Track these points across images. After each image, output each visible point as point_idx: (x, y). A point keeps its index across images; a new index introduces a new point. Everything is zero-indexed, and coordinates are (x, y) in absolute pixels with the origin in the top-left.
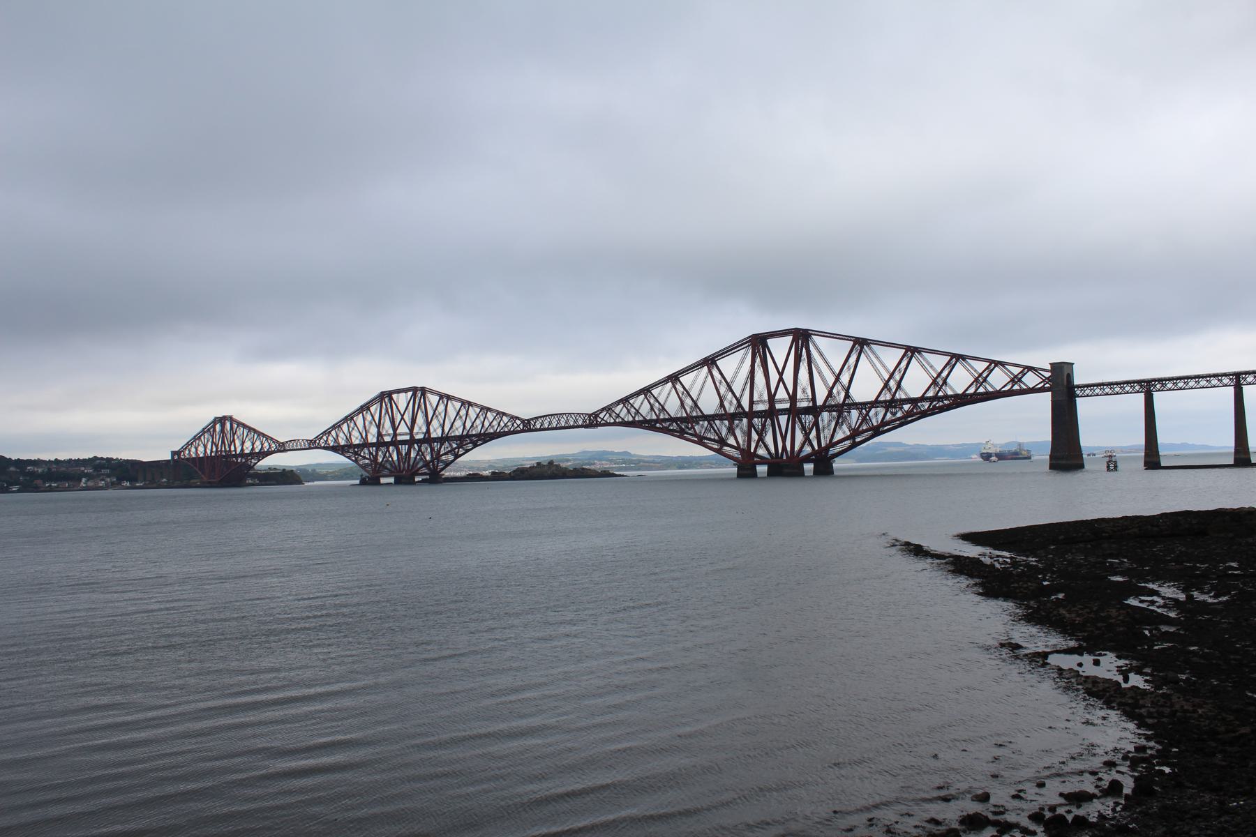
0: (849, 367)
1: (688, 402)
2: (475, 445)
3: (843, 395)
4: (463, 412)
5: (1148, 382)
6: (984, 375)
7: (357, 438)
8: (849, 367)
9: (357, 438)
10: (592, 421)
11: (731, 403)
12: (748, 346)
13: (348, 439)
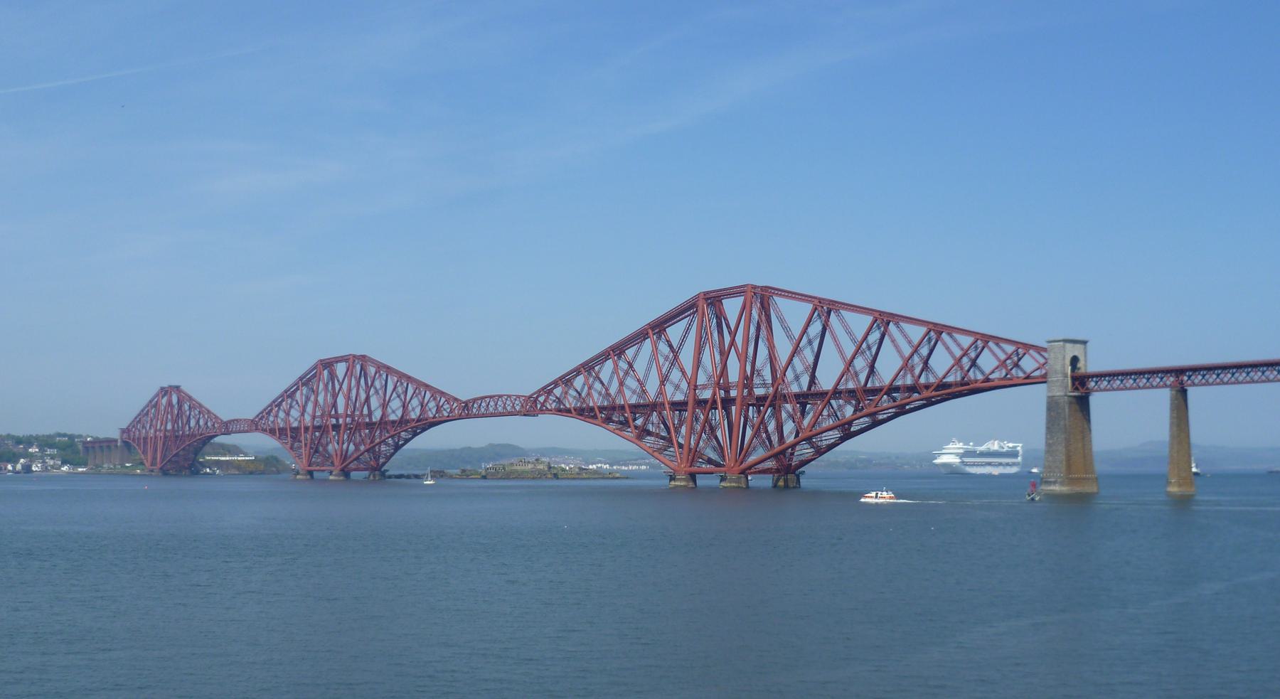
0: (810, 342)
1: (631, 383)
2: (415, 435)
3: (805, 380)
4: (400, 389)
5: (1179, 372)
6: (973, 355)
7: (296, 420)
8: (810, 342)
9: (296, 420)
10: (531, 406)
11: (677, 387)
12: (694, 313)
13: (286, 421)
